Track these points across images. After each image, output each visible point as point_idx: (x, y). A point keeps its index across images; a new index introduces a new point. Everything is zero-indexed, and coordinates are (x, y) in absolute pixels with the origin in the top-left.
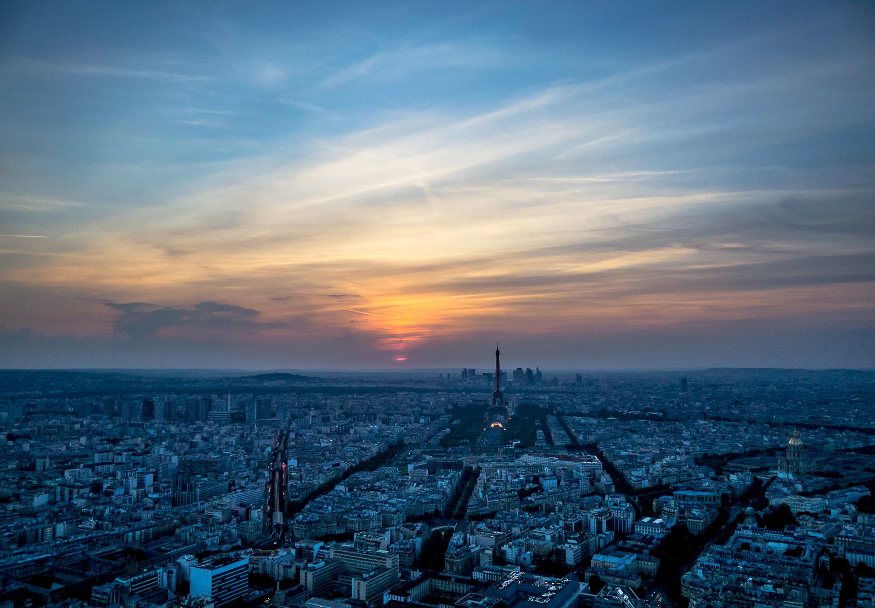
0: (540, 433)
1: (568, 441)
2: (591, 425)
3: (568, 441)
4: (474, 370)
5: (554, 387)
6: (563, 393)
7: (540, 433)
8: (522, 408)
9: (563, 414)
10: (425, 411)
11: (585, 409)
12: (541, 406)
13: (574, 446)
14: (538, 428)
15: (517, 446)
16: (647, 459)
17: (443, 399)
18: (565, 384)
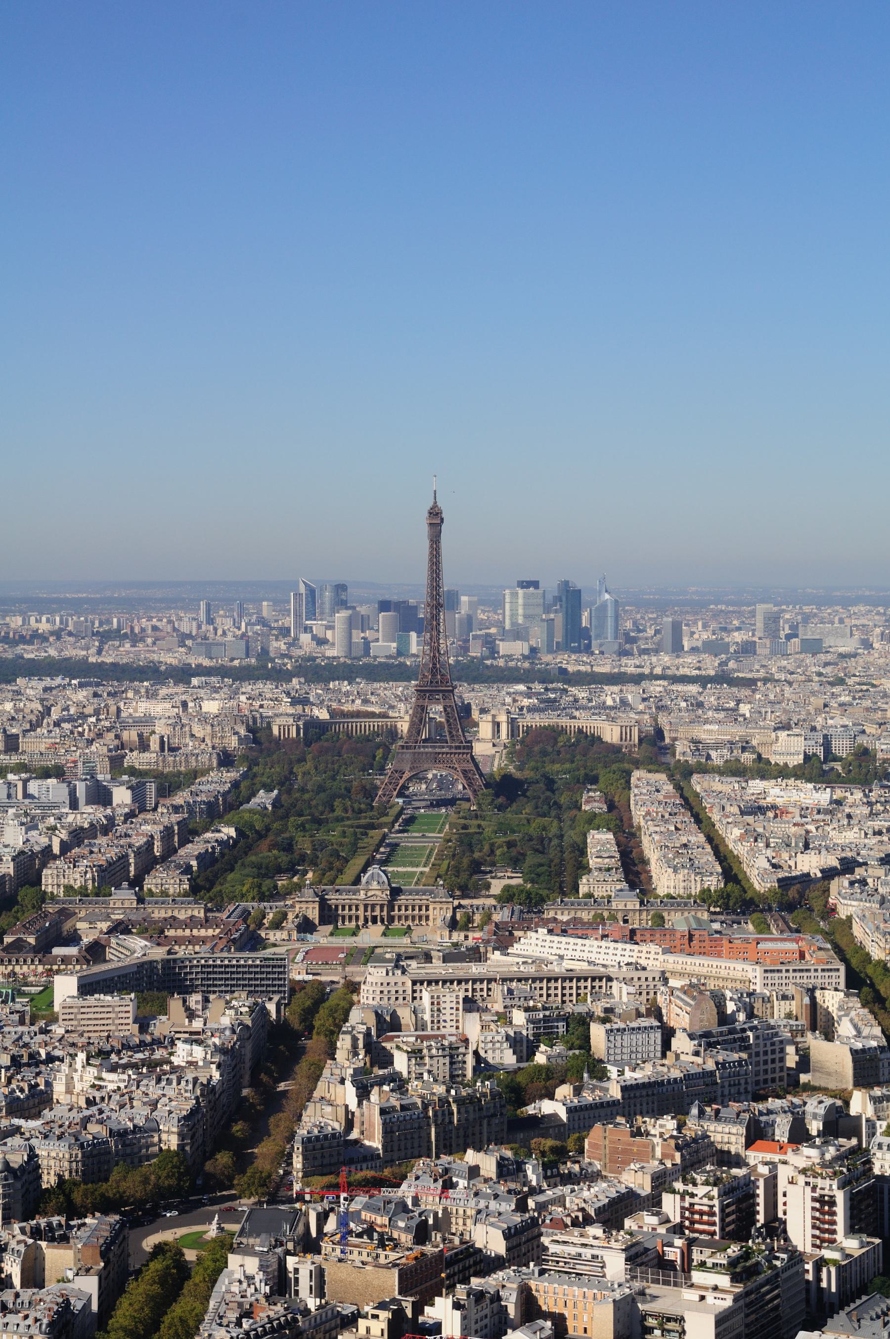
0: (601, 843)
1: (714, 882)
2: (804, 811)
3: (714, 882)
4: (340, 588)
5: (666, 659)
6: (703, 681)
7: (601, 843)
8: (532, 744)
9: (704, 769)
10: (134, 759)
11: (789, 749)
12: (611, 734)
13: (735, 900)
14: (592, 821)
15: (508, 896)
17: (211, 707)
18: (713, 648)
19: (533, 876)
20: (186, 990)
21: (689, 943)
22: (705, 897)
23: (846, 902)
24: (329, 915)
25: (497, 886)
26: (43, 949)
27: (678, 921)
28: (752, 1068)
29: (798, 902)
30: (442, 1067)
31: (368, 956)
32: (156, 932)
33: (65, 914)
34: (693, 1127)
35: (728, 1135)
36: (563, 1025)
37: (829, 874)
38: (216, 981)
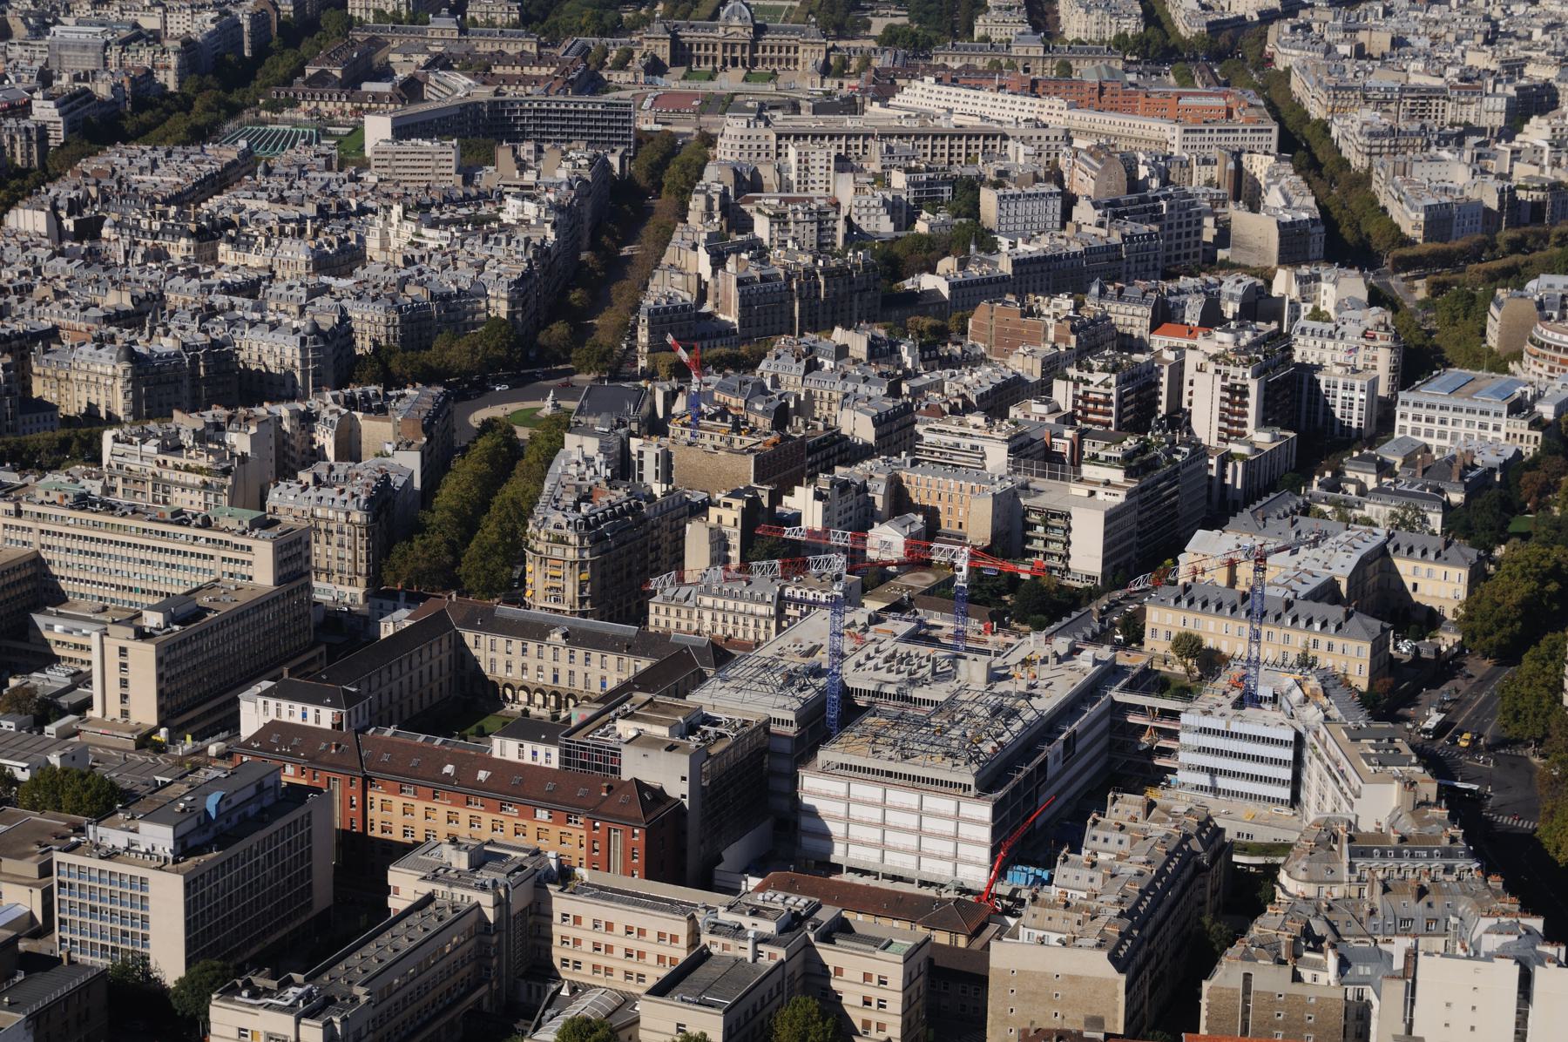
1: (1131, 26)
3: (1131, 26)
13: (1156, 47)
15: (890, 38)
16: (1491, 111)
19: (919, 16)
20: (516, 138)
21: (1100, 97)
22: (1121, 43)
23: (1285, 51)
24: (682, 54)
25: (878, 26)
26: (350, 84)
27: (1087, 71)
28: (1164, 241)
29: (1230, 49)
30: (809, 234)
31: (726, 104)
32: (480, 68)
33: (376, 44)
34: (1092, 305)
35: (1131, 317)
36: (950, 188)
37: (1268, 17)
38: (551, 129)
